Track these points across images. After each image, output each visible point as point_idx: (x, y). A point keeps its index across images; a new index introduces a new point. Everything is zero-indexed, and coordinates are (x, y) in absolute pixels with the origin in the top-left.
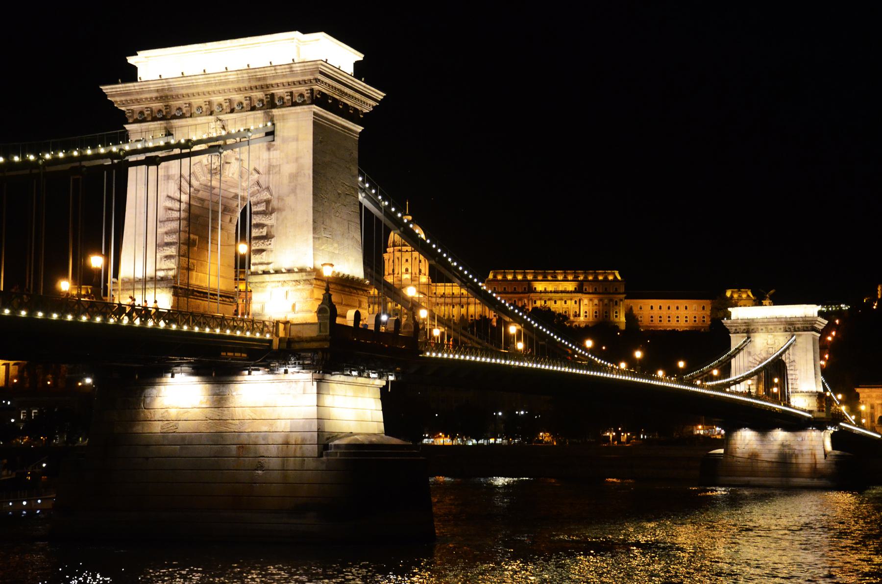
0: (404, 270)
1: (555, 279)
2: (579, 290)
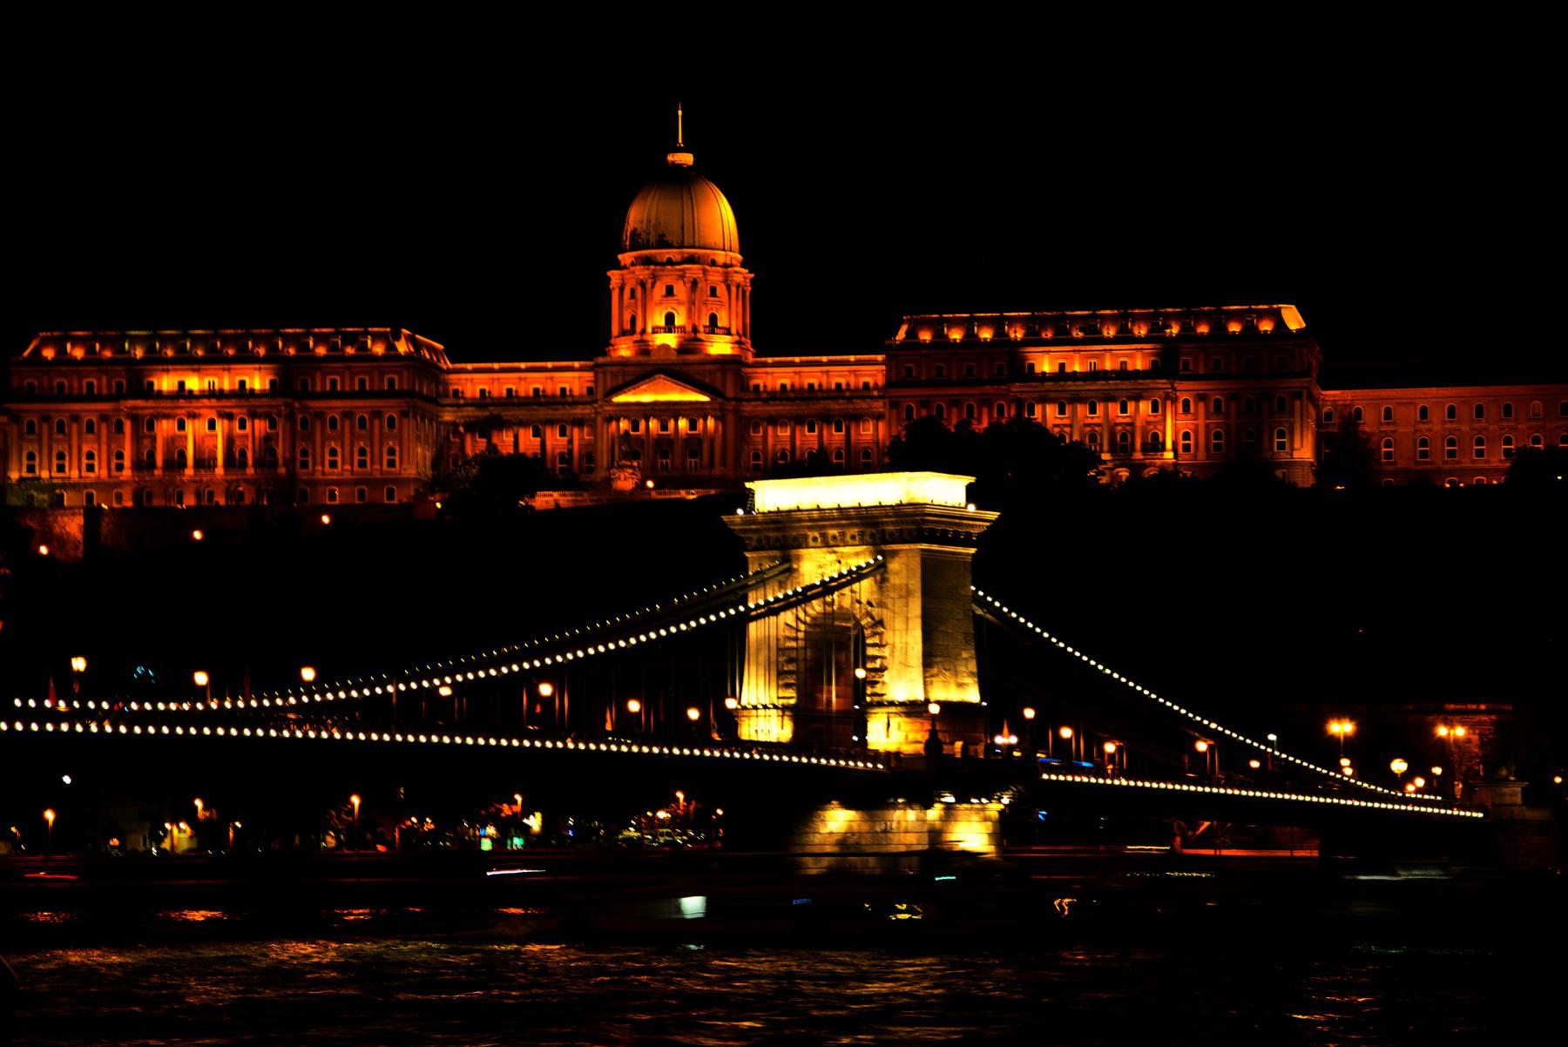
0: (660, 321)
1: (1093, 338)
2: (1168, 365)
